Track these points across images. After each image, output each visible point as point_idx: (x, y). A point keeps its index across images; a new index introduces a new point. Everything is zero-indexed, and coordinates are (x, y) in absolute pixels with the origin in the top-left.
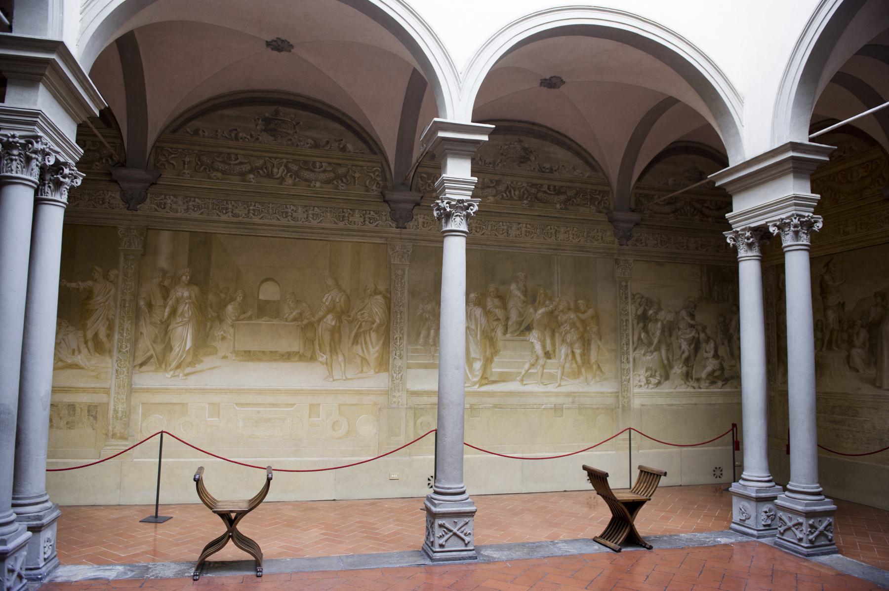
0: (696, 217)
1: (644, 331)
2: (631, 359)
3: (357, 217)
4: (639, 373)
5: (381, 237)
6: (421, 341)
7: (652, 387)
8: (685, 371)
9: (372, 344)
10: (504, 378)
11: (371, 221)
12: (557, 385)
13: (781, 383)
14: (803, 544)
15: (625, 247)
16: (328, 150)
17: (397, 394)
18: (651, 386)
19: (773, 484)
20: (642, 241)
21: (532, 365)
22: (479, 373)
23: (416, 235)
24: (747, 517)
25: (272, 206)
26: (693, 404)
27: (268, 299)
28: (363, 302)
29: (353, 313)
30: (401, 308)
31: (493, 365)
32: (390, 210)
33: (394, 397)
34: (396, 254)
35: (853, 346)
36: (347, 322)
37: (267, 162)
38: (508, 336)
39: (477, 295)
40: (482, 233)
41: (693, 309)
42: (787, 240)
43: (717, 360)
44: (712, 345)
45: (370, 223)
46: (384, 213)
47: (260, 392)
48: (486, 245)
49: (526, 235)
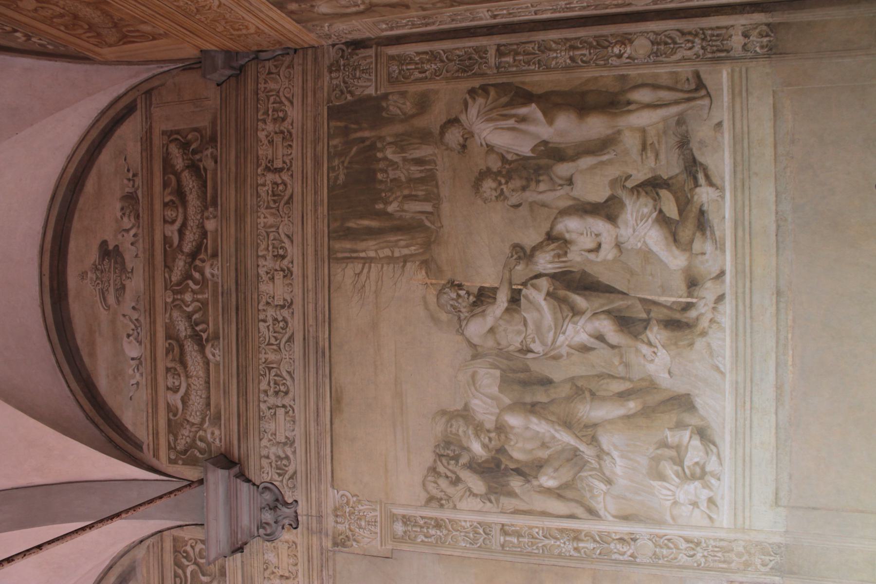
0: (208, 271)
1: (536, 477)
2: (624, 528)
4: (669, 503)
7: (714, 458)
15: (301, 509)
18: (712, 465)
20: (283, 456)
26: (778, 303)
41: (462, 293)
43: (622, 205)
44: (571, 225)
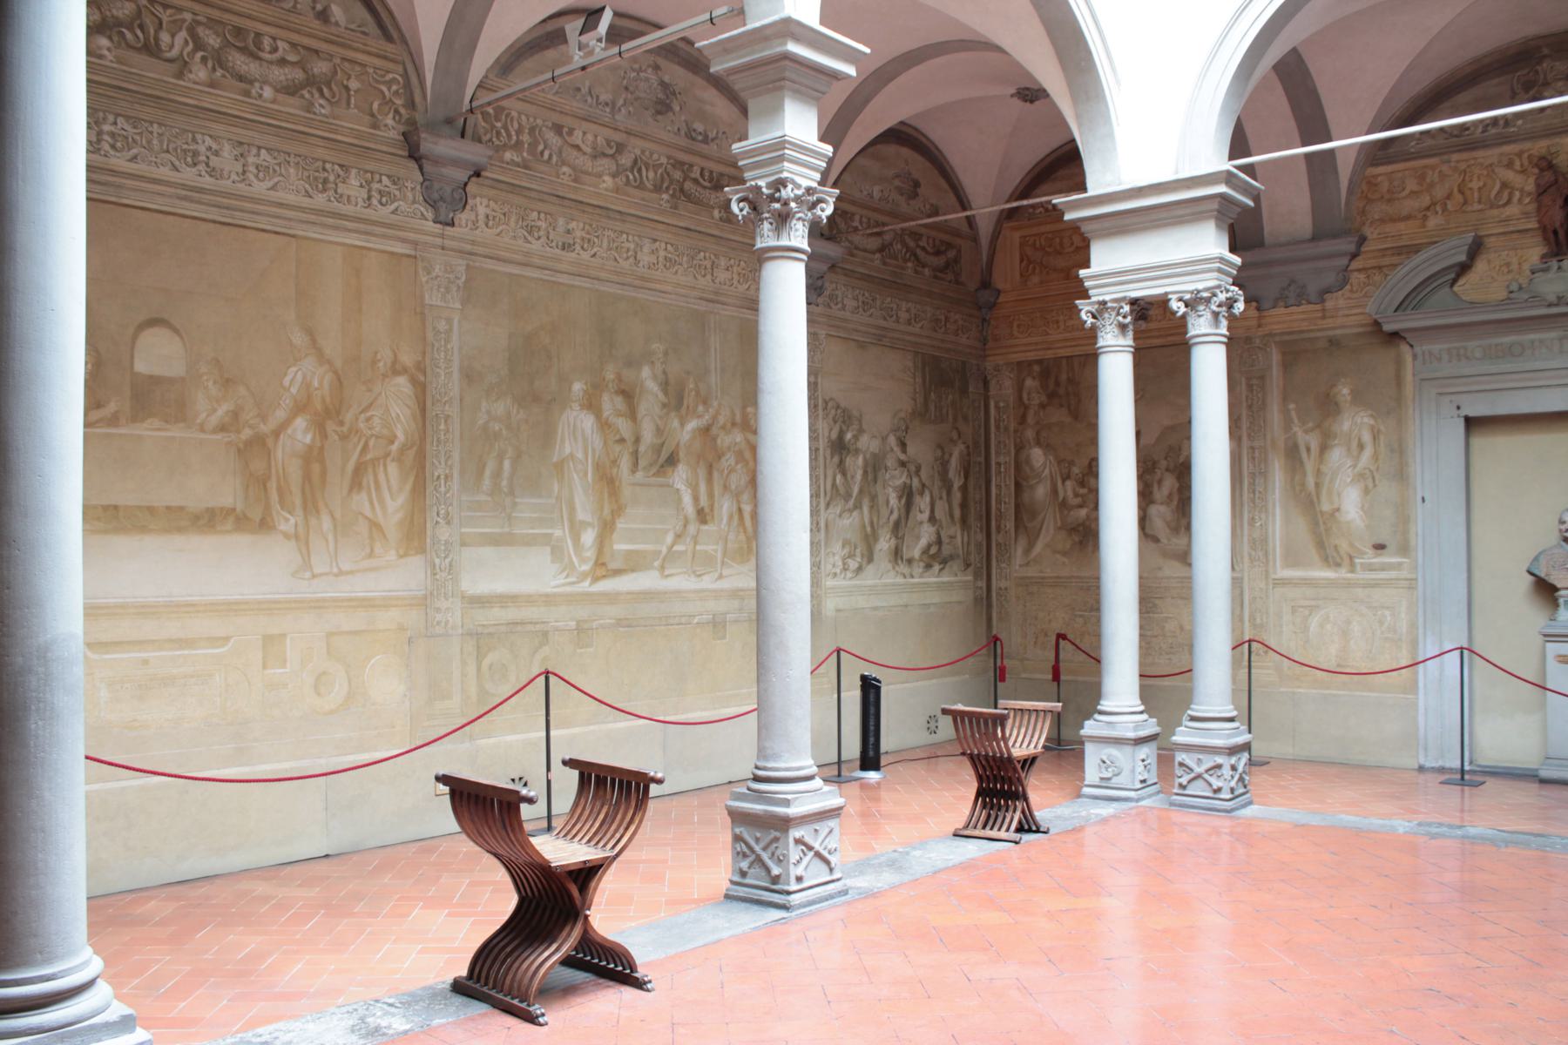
0: (910, 264)
2: (822, 525)
3: (353, 186)
5: (404, 241)
6: (487, 482)
8: (893, 547)
9: (389, 488)
10: (634, 563)
11: (384, 200)
12: (716, 575)
13: (1020, 566)
14: (1222, 796)
16: (289, 11)
17: (443, 604)
18: (849, 575)
19: (1145, 716)
21: (678, 536)
22: (590, 554)
23: (473, 243)
24: (1116, 772)
25: (160, 131)
27: (157, 371)
28: (370, 390)
29: (348, 417)
30: (447, 407)
31: (615, 536)
32: (421, 179)
33: (438, 610)
34: (436, 282)
35: (1152, 502)
36: (336, 437)
37: (143, 10)
38: (640, 475)
39: (585, 387)
40: (593, 252)
42: (1200, 325)
43: (934, 526)
44: (927, 499)
45: (382, 204)
46: (409, 184)
47: (145, 611)
48: (598, 279)
49: (665, 266)
